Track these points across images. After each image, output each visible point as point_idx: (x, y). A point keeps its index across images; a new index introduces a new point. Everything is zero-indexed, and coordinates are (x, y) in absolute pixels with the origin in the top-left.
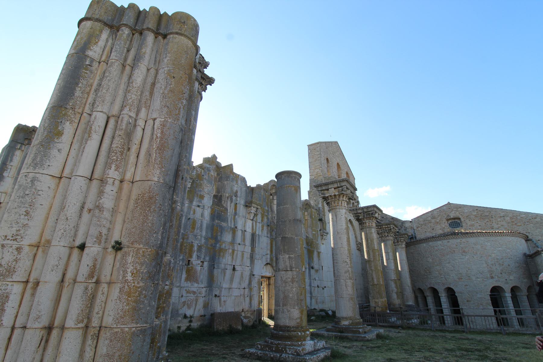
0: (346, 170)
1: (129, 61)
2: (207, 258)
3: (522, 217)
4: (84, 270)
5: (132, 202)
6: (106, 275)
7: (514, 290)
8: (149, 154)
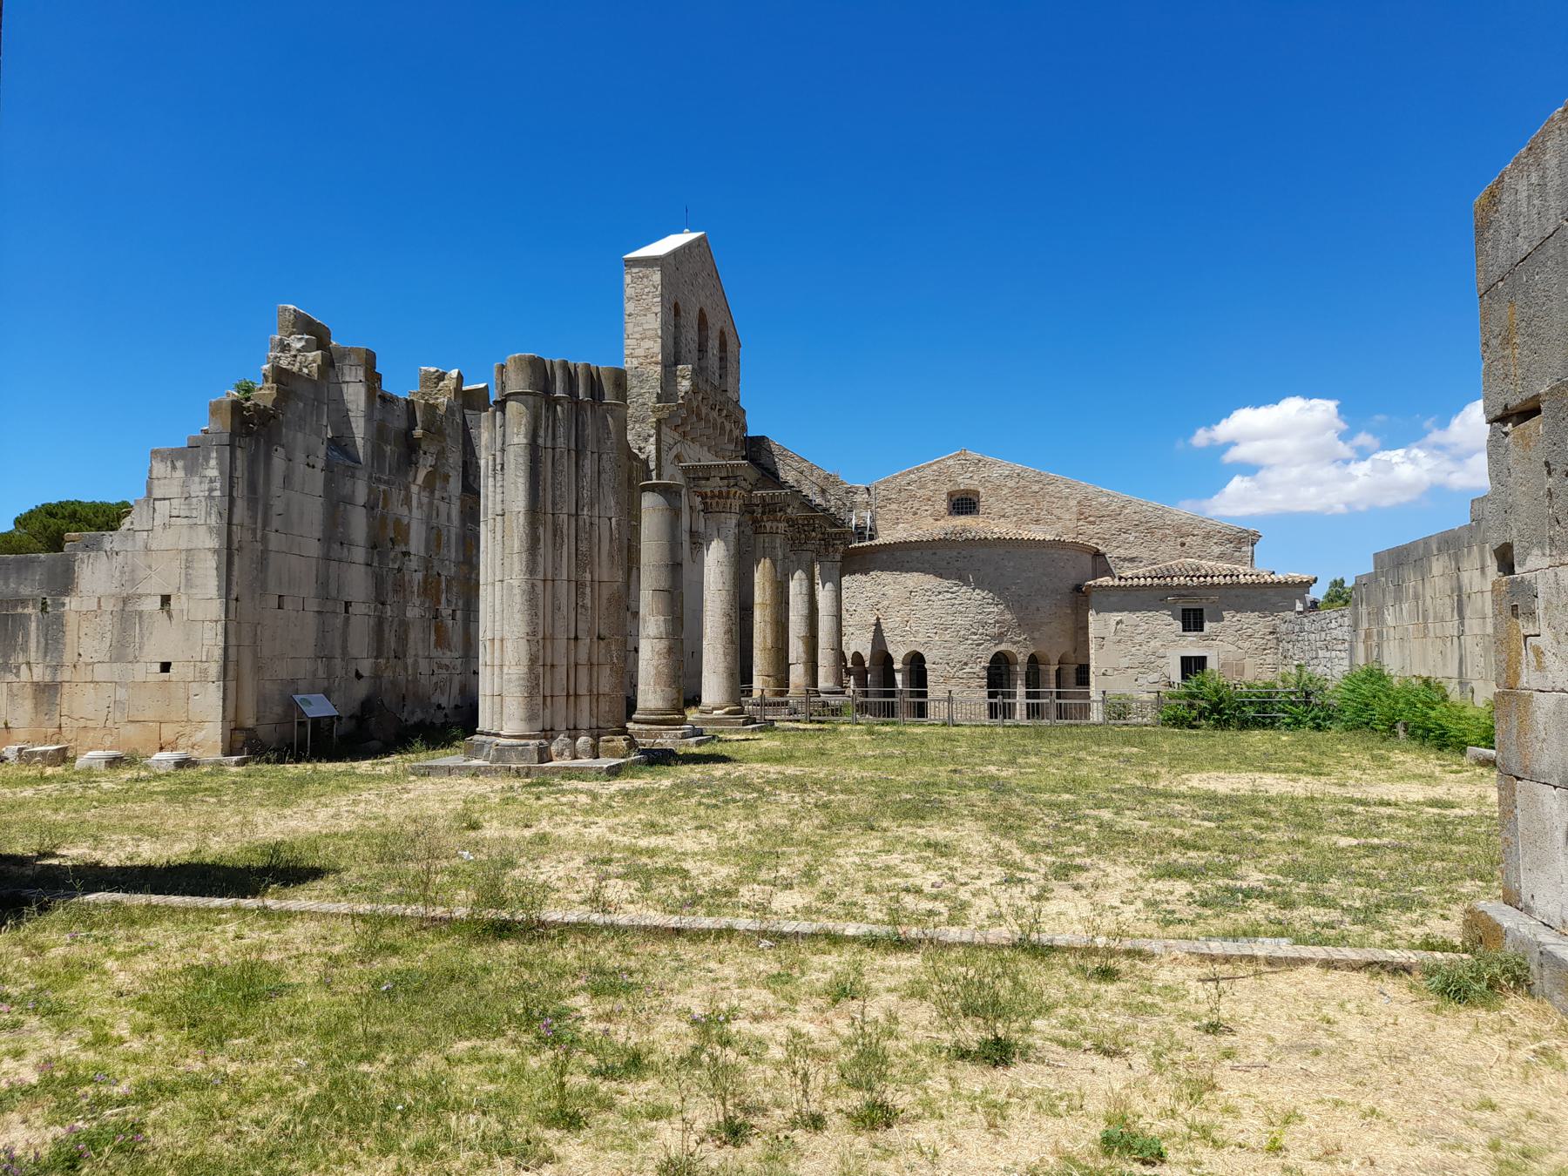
1: (573, 446)
2: (460, 603)
4: (583, 658)
5: (604, 602)
6: (595, 661)
7: (1033, 660)
8: (611, 556)
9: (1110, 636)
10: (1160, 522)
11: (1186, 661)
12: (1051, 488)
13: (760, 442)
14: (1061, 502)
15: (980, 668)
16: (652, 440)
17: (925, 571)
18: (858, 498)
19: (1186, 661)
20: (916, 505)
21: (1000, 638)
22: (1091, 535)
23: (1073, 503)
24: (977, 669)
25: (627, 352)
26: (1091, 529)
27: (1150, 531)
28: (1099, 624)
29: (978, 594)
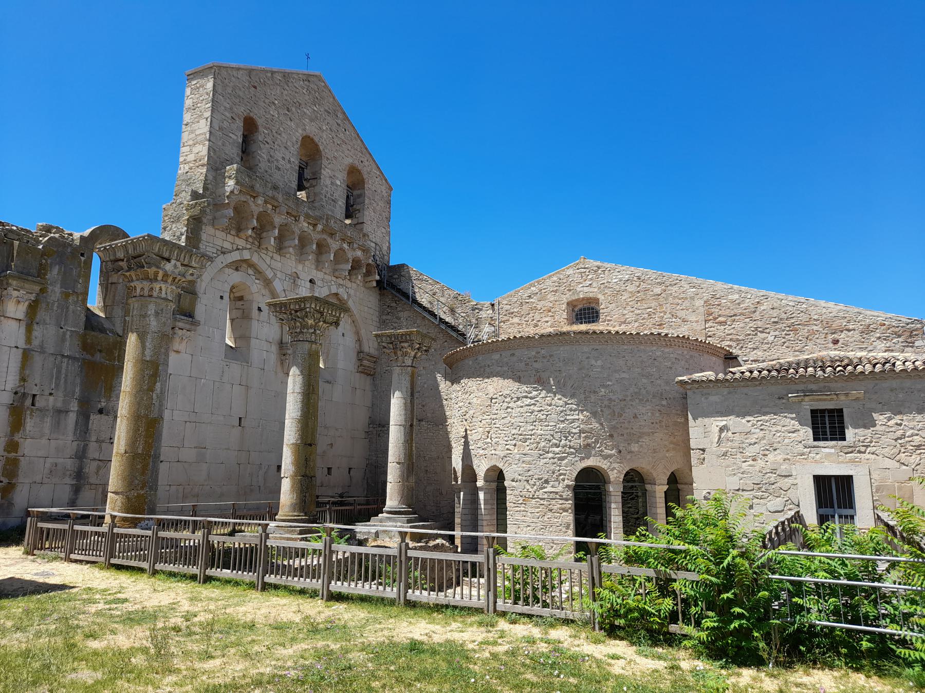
0: (349, 161)
3: (733, 302)
9: (712, 448)
10: (804, 318)
11: (821, 482)
12: (675, 289)
13: (401, 267)
14: (687, 303)
15: (564, 486)
16: (184, 237)
17: (503, 376)
18: (483, 314)
19: (821, 482)
20: (537, 317)
21: (586, 450)
22: (720, 337)
23: (699, 303)
24: (560, 489)
25: (181, 159)
26: (720, 331)
27: (793, 328)
28: (704, 431)
29: (559, 400)
